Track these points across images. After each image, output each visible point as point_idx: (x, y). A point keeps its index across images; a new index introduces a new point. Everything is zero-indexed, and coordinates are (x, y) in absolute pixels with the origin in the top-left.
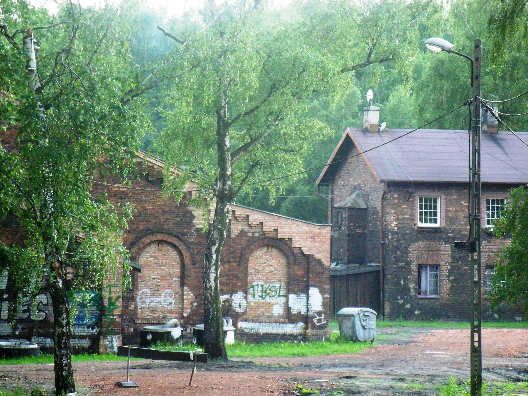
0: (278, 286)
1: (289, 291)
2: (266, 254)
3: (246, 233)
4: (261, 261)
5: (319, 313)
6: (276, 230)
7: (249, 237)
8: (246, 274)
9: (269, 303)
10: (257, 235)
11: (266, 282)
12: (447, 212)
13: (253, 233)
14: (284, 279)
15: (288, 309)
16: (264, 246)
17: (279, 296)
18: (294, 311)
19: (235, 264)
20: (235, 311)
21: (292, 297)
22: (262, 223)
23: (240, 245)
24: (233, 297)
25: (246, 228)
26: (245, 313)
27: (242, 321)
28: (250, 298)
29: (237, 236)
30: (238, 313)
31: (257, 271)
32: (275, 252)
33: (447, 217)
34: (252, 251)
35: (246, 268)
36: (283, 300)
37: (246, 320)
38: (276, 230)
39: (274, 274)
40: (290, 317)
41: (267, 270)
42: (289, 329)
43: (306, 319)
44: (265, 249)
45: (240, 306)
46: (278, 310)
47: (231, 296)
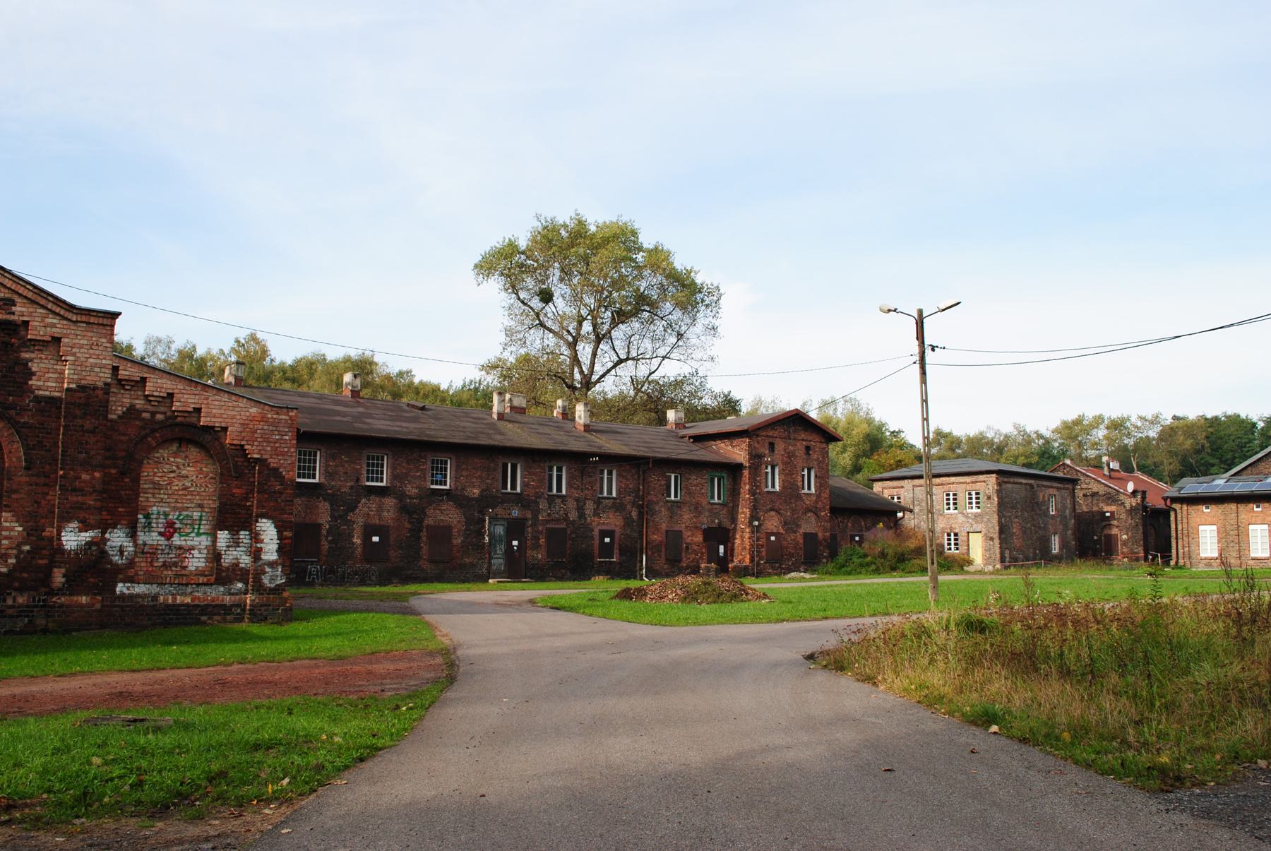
0: (196, 515)
1: (220, 524)
2: (176, 455)
3: (140, 412)
4: (166, 468)
5: (272, 564)
6: (198, 410)
7: (144, 419)
8: (136, 491)
9: (180, 548)
10: (160, 417)
11: (175, 509)
12: (327, 466)
13: (153, 414)
14: (212, 504)
15: (215, 556)
16: (172, 441)
17: (198, 534)
18: (227, 560)
19: (113, 471)
20: (111, 562)
21: (223, 536)
22: (171, 395)
23: (124, 435)
24: (107, 535)
25: (140, 403)
26: (131, 563)
27: (124, 582)
28: (142, 537)
29: (120, 417)
30: (117, 565)
31: (158, 487)
32: (193, 452)
33: (326, 471)
34: (152, 449)
35: (137, 480)
36: (205, 541)
37: (132, 580)
38: (198, 410)
39: (191, 493)
40: (220, 573)
41: (177, 485)
42: (216, 593)
43: (252, 577)
44: (175, 447)
45: (121, 552)
46: (197, 562)
47: (104, 533)
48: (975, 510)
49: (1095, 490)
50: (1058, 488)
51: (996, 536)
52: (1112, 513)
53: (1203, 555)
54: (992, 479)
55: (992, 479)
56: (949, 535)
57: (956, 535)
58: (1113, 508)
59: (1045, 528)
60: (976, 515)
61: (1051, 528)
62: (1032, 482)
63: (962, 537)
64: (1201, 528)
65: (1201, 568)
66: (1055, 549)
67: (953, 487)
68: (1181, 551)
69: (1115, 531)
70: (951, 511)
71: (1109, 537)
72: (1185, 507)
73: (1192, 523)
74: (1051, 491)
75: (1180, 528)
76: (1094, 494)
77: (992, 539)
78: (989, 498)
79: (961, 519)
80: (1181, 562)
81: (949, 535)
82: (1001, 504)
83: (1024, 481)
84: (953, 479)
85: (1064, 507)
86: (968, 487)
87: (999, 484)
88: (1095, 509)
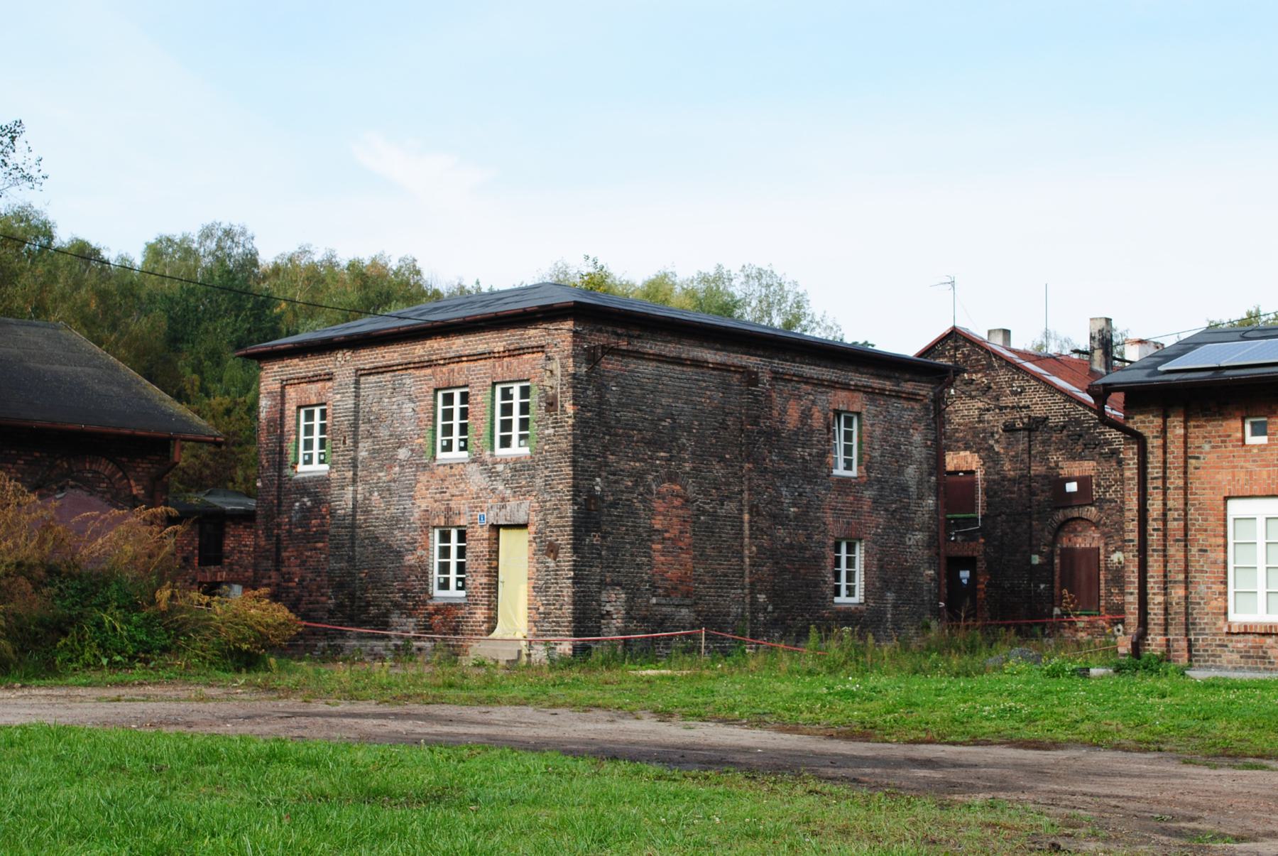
48: (518, 450)
49: (1038, 411)
50: (871, 393)
51: (564, 539)
52: (1084, 482)
53: (1237, 617)
54: (561, 336)
55: (561, 336)
56: (445, 537)
57: (462, 536)
58: (1087, 467)
59: (805, 519)
60: (519, 467)
61: (833, 525)
62: (751, 361)
63: (478, 546)
64: (1236, 508)
65: (1228, 667)
66: (852, 596)
67: (461, 372)
68: (1155, 599)
69: (1086, 540)
70: (456, 454)
71: (1070, 555)
72: (1177, 429)
73: (1204, 494)
74: (840, 399)
75: (1155, 507)
76: (1036, 425)
77: (552, 550)
78: (551, 405)
79: (477, 479)
80: (1155, 642)
81: (445, 537)
82: (580, 422)
83: (710, 356)
84: (458, 344)
85: (899, 457)
86: (501, 369)
87: (591, 357)
88: (1037, 469)
